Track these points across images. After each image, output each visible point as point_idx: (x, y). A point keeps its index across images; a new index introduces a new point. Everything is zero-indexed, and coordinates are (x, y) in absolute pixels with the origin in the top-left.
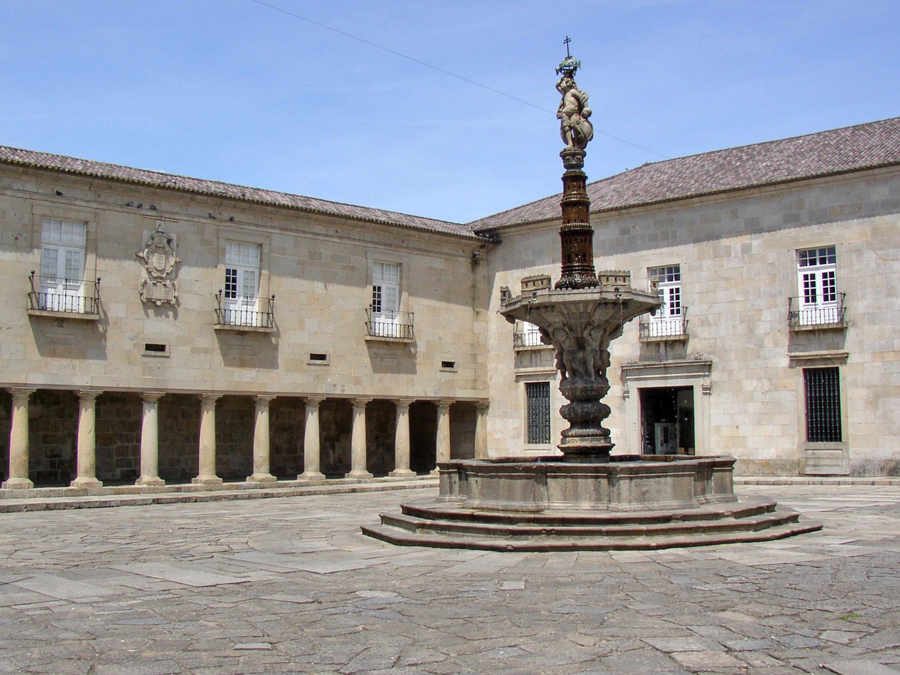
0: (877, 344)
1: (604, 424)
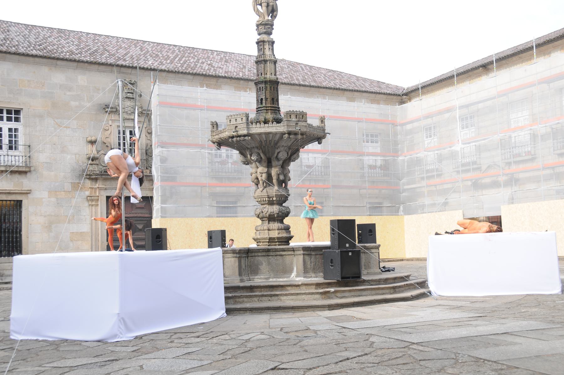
0: (52, 186)
1: (287, 221)
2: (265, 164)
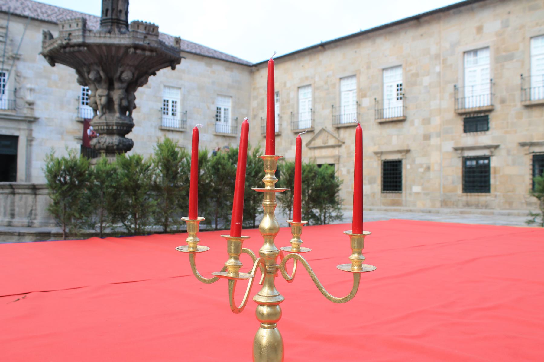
2: (105, 86)
